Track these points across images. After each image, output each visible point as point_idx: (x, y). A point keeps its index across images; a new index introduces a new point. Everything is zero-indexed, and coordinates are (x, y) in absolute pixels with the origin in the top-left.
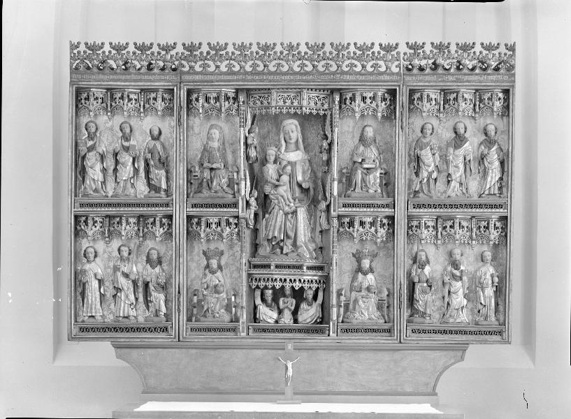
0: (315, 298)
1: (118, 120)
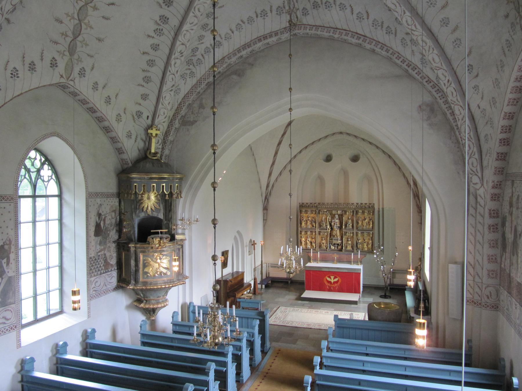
0: (341, 245)
1: (307, 215)
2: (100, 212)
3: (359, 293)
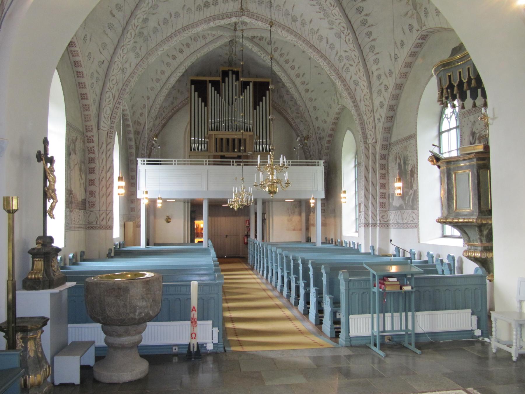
2: (474, 130)
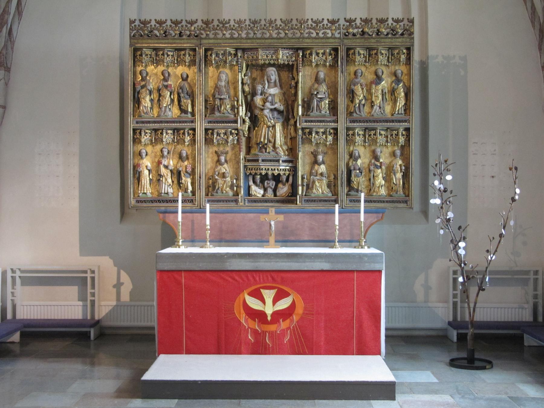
0: (287, 180)
1: (161, 68)
3: (379, 353)
